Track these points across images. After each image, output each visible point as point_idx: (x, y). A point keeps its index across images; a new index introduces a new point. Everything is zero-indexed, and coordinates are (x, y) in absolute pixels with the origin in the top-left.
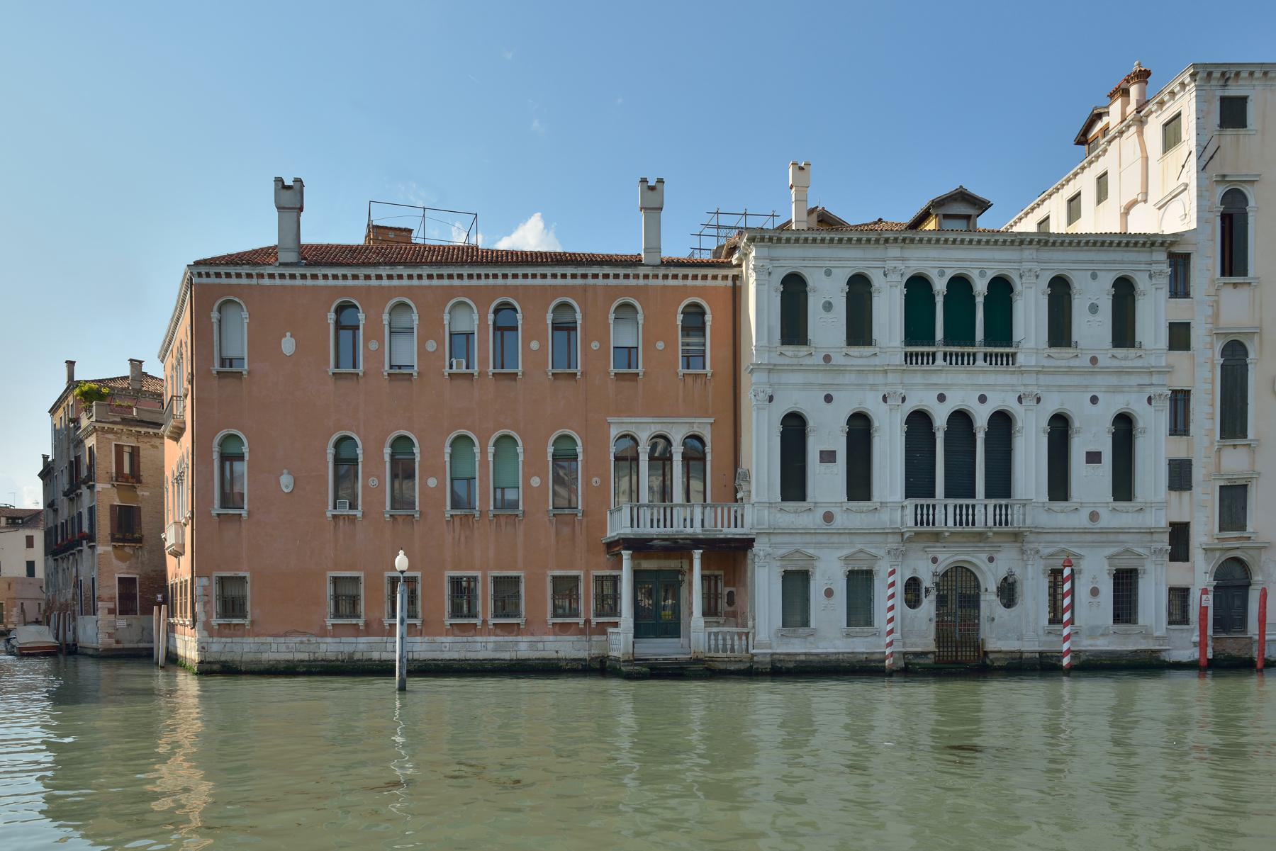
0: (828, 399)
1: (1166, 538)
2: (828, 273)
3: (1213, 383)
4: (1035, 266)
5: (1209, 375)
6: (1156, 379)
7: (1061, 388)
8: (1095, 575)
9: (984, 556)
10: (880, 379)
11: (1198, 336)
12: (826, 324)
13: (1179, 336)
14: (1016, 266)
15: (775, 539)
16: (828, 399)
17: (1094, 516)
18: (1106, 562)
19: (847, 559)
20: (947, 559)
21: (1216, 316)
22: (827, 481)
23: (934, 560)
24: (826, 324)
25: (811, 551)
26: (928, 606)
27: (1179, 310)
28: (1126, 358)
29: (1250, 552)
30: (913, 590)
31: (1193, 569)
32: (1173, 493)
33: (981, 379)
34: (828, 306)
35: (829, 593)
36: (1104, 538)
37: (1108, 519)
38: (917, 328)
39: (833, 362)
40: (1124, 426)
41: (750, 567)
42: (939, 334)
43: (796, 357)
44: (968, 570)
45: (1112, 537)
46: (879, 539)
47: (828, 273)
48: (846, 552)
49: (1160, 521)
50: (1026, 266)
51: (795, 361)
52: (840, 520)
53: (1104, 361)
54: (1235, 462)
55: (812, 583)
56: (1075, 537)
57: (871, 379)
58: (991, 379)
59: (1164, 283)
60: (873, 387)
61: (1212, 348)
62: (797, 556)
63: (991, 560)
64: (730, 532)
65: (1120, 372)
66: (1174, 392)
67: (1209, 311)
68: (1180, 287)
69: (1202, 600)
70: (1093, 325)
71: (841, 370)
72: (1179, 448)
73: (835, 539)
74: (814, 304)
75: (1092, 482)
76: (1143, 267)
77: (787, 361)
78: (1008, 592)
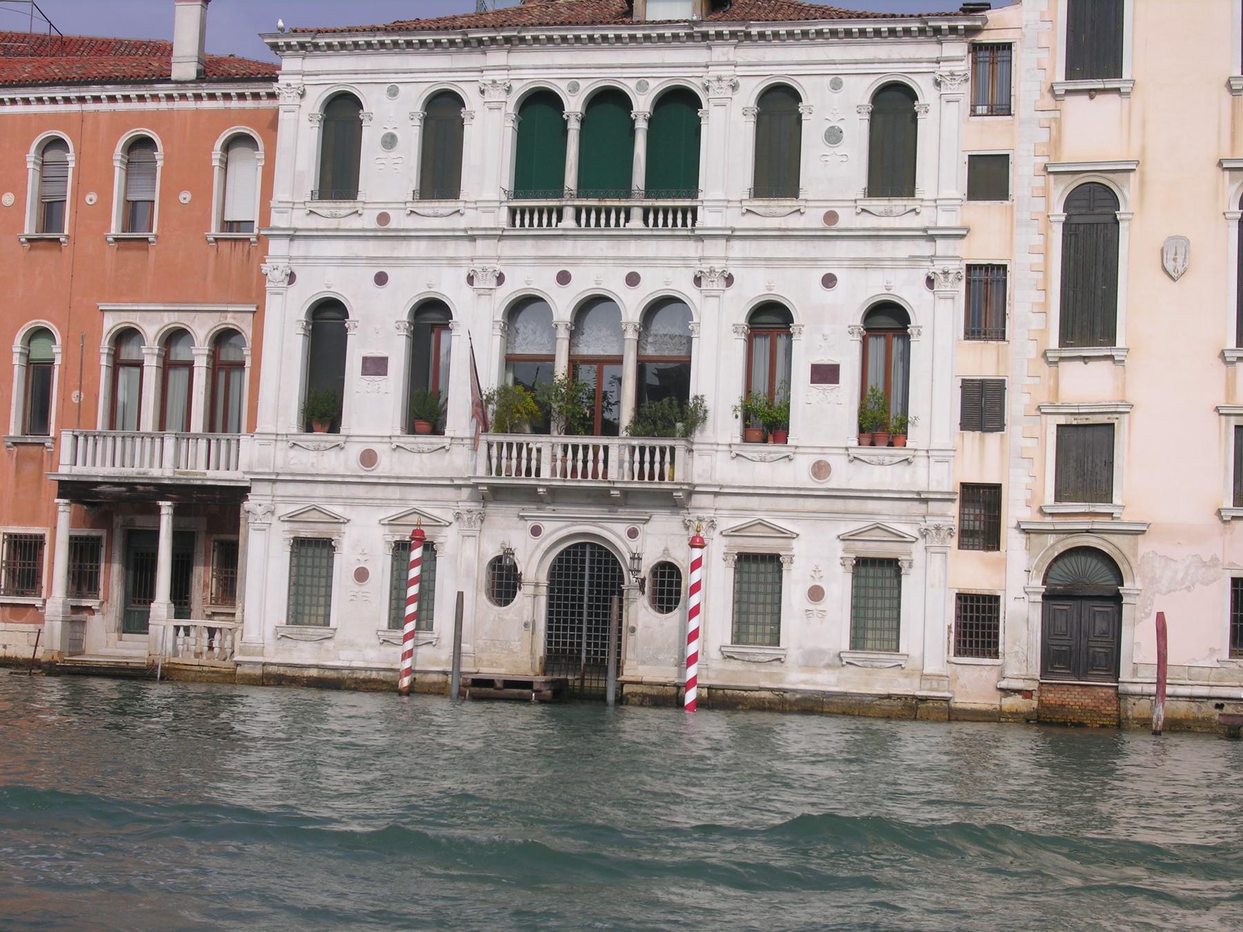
0: (381, 279)
1: (954, 509)
2: (393, 92)
3: (1046, 254)
4: (726, 72)
5: (1038, 240)
6: (942, 247)
7: (769, 262)
8: (817, 565)
9: (622, 528)
10: (465, 249)
11: (1022, 176)
12: (390, 169)
13: (988, 177)
14: (699, 72)
15: (281, 489)
16: (381, 279)
17: (820, 469)
18: (841, 545)
19: (393, 523)
20: (560, 527)
21: (1056, 143)
22: (373, 404)
23: (536, 531)
24: (390, 169)
25: (337, 510)
26: (531, 605)
27: (990, 136)
28: (888, 214)
29: (1114, 539)
30: (503, 580)
31: (1003, 563)
32: (972, 437)
33: (632, 249)
34: (390, 141)
35: (361, 575)
36: (839, 505)
37: (843, 475)
38: (535, 169)
39: (393, 224)
40: (887, 321)
41: (242, 530)
42: (571, 180)
43: (335, 217)
44: (600, 547)
45: (852, 505)
46: (450, 493)
47: (393, 92)
48: (393, 512)
49: (946, 479)
50: (714, 72)
51: (333, 223)
52: (387, 464)
53: (847, 219)
54: (1086, 384)
55: (337, 558)
56: (784, 503)
57: (451, 249)
58: (651, 248)
59: (964, 91)
60: (453, 261)
61: (1046, 196)
62: (314, 516)
63: (633, 534)
64: (219, 476)
65: (875, 236)
66: (969, 267)
67: (1044, 136)
68: (993, 97)
69: (1021, 623)
70: (834, 161)
71: (403, 237)
72: (981, 361)
73: (379, 492)
74: (370, 137)
75: (824, 416)
76: (924, 67)
77: (322, 223)
78: (667, 586)
